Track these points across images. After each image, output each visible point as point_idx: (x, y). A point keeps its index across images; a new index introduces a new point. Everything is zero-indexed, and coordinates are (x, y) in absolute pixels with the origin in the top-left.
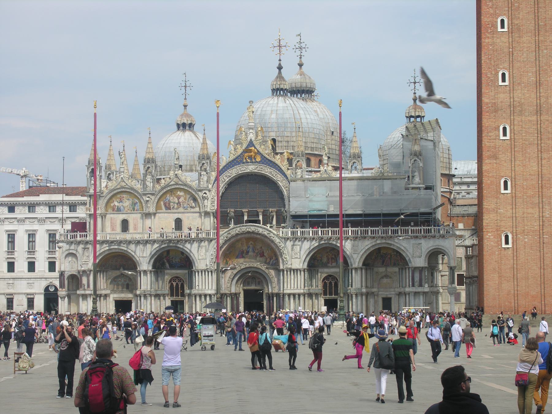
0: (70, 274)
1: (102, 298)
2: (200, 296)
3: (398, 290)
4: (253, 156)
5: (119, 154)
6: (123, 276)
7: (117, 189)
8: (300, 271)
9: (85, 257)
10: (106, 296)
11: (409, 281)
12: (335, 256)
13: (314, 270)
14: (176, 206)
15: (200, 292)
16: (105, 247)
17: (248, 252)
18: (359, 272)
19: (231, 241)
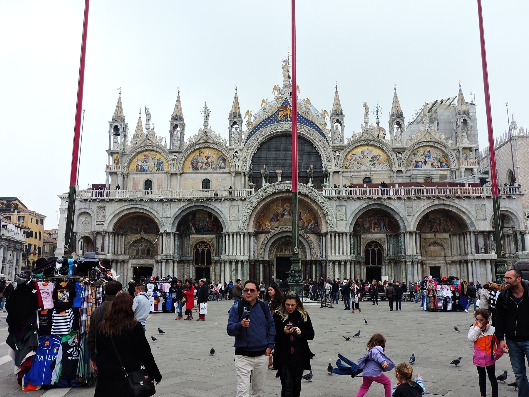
0: (83, 235)
1: (119, 264)
2: (231, 263)
3: (449, 259)
4: (289, 115)
5: (145, 110)
6: (143, 240)
7: (141, 147)
8: (346, 235)
9: (100, 218)
10: (123, 261)
11: (471, 247)
12: (378, 221)
13: (356, 236)
14: (204, 166)
15: (231, 258)
16: (125, 206)
17: (283, 215)
18: (414, 236)
19: (266, 201)
